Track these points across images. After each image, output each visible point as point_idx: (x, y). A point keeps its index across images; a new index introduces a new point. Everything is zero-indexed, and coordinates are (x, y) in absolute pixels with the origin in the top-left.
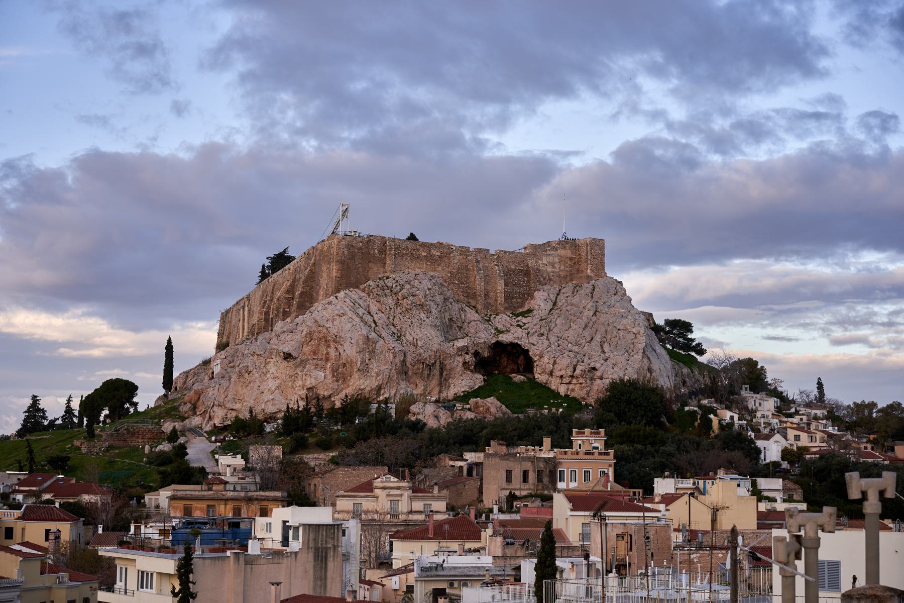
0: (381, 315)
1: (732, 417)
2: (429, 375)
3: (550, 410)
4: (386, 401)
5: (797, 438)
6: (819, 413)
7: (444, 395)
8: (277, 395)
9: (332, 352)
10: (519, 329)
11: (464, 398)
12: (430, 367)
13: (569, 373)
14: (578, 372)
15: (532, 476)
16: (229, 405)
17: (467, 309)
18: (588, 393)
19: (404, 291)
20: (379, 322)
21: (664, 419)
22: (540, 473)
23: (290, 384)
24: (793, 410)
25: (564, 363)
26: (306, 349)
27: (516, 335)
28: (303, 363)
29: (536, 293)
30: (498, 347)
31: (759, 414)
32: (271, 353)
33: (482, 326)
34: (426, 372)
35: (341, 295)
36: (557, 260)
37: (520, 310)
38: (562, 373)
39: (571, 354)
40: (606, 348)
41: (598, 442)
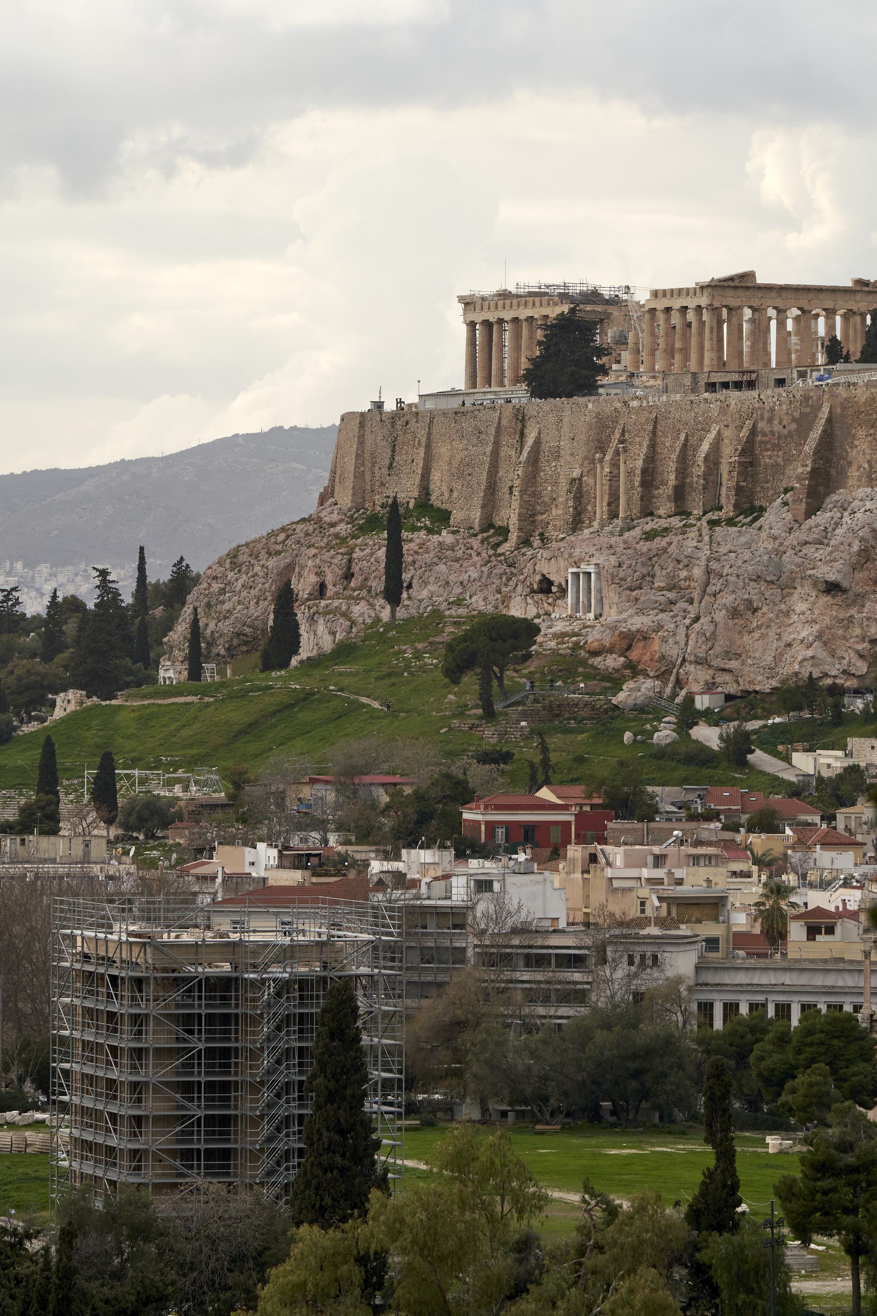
8: (817, 650)
16: (717, 662)
23: (840, 632)
26: (859, 575)
28: (859, 599)
32: (794, 580)
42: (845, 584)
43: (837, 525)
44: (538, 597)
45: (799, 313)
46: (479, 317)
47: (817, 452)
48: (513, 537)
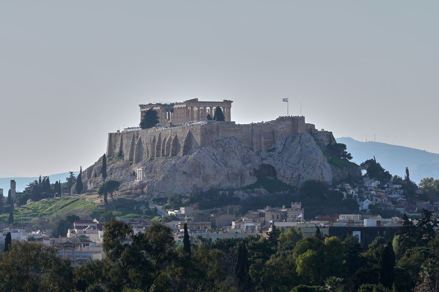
0: (218, 155)
1: (353, 192)
2: (237, 178)
3: (283, 192)
4: (226, 190)
5: (376, 200)
6: (398, 186)
7: (242, 186)
9: (202, 171)
10: (270, 158)
11: (251, 187)
12: (237, 175)
13: (291, 177)
14: (294, 176)
15: (280, 217)
16: (160, 191)
17: (250, 150)
18: (298, 184)
19: (227, 146)
20: (218, 158)
21: (325, 194)
22: (282, 216)
24: (386, 186)
25: (289, 172)
27: (269, 161)
29: (277, 141)
30: (263, 166)
31: (369, 189)
33: (256, 157)
34: (236, 177)
35: (203, 148)
36: (285, 126)
37: (270, 149)
38: (287, 177)
39: (291, 169)
40: (305, 165)
41: (299, 206)
42: (187, 172)
43: (188, 158)
44: (133, 176)
45: (210, 108)
46: (143, 110)
47: (185, 141)
48: (134, 162)
